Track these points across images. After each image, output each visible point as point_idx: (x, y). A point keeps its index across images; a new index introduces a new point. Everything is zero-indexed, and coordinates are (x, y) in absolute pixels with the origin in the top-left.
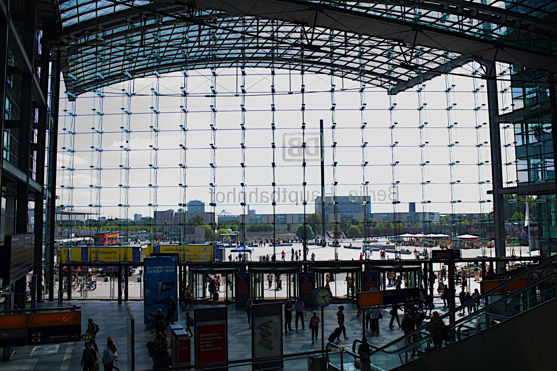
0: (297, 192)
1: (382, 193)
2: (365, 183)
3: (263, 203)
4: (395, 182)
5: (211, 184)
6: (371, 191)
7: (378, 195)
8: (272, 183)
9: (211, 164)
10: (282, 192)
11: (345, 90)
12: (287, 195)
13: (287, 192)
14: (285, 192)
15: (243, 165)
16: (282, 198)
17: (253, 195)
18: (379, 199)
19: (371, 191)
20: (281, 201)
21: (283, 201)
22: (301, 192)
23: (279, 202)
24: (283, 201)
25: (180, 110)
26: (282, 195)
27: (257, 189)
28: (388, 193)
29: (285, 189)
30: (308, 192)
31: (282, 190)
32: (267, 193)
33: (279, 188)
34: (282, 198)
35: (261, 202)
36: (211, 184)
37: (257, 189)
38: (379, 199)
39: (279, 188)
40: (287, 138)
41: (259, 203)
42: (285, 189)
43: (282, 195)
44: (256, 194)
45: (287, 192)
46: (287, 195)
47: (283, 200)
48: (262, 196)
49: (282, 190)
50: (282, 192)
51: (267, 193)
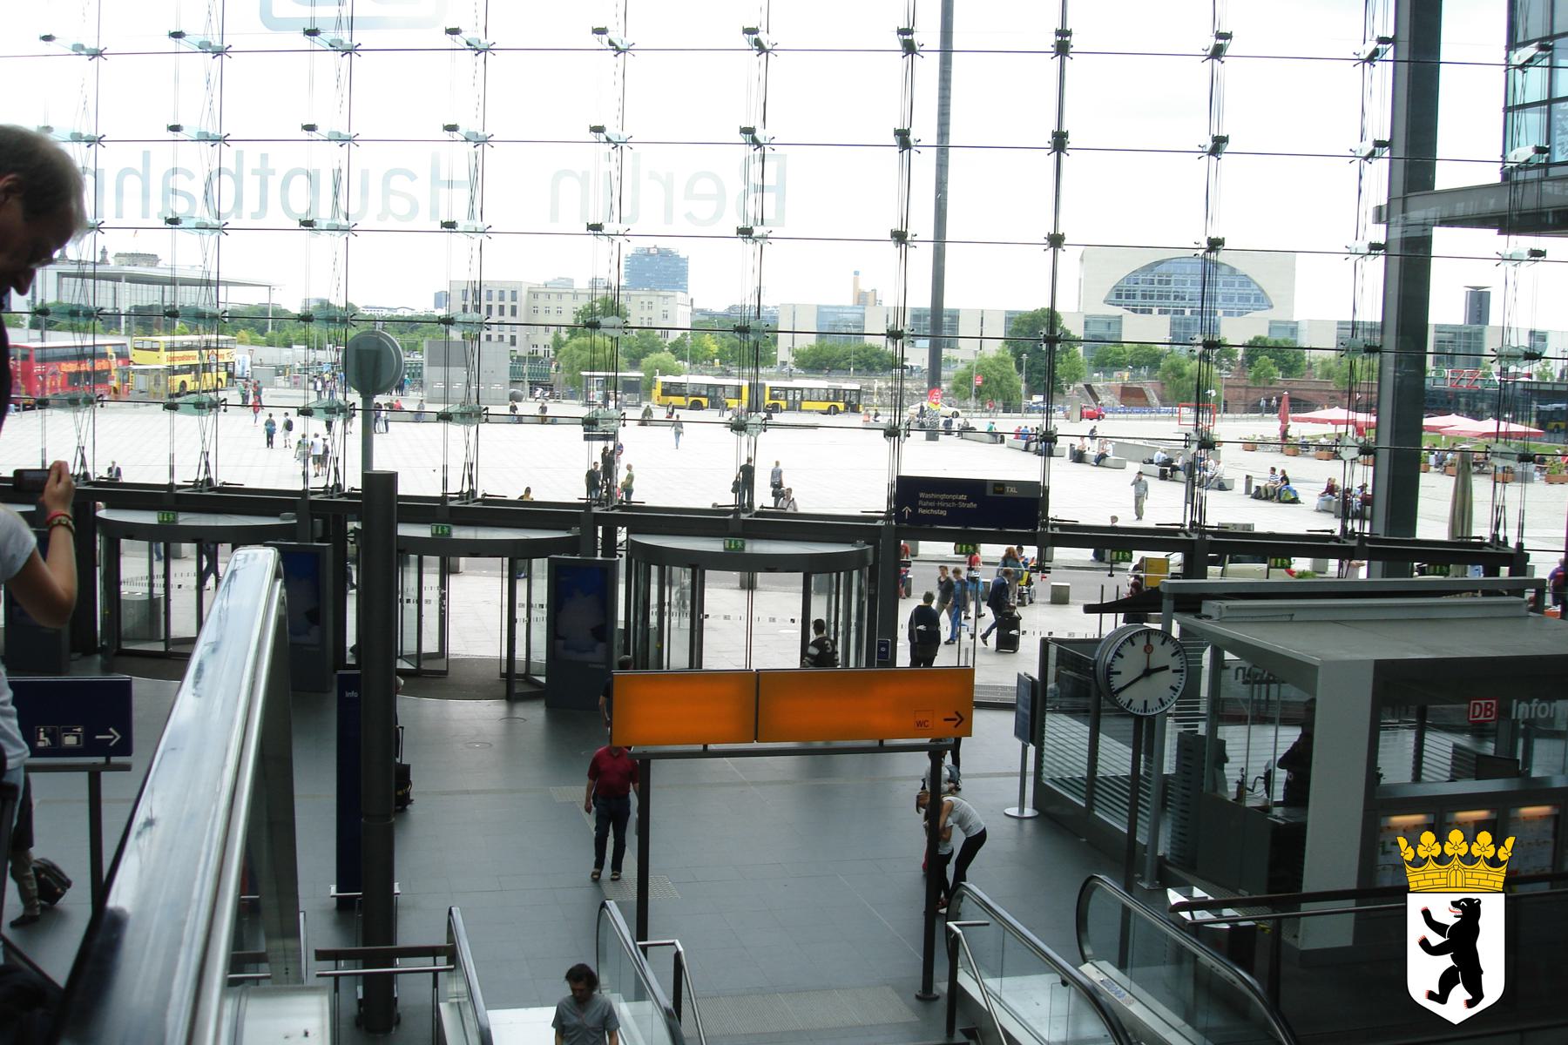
10: (254, 172)
13: (273, 173)
14: (264, 175)
16: (251, 202)
17: (132, 185)
18: (690, 216)
21: (254, 216)
23: (239, 217)
24: (254, 216)
27: (146, 155)
28: (735, 187)
29: (264, 157)
30: (365, 174)
33: (240, 154)
34: (251, 202)
37: (146, 155)
38: (690, 216)
39: (240, 154)
42: (264, 157)
44: (145, 179)
45: (273, 173)
47: (256, 208)
50: (254, 172)
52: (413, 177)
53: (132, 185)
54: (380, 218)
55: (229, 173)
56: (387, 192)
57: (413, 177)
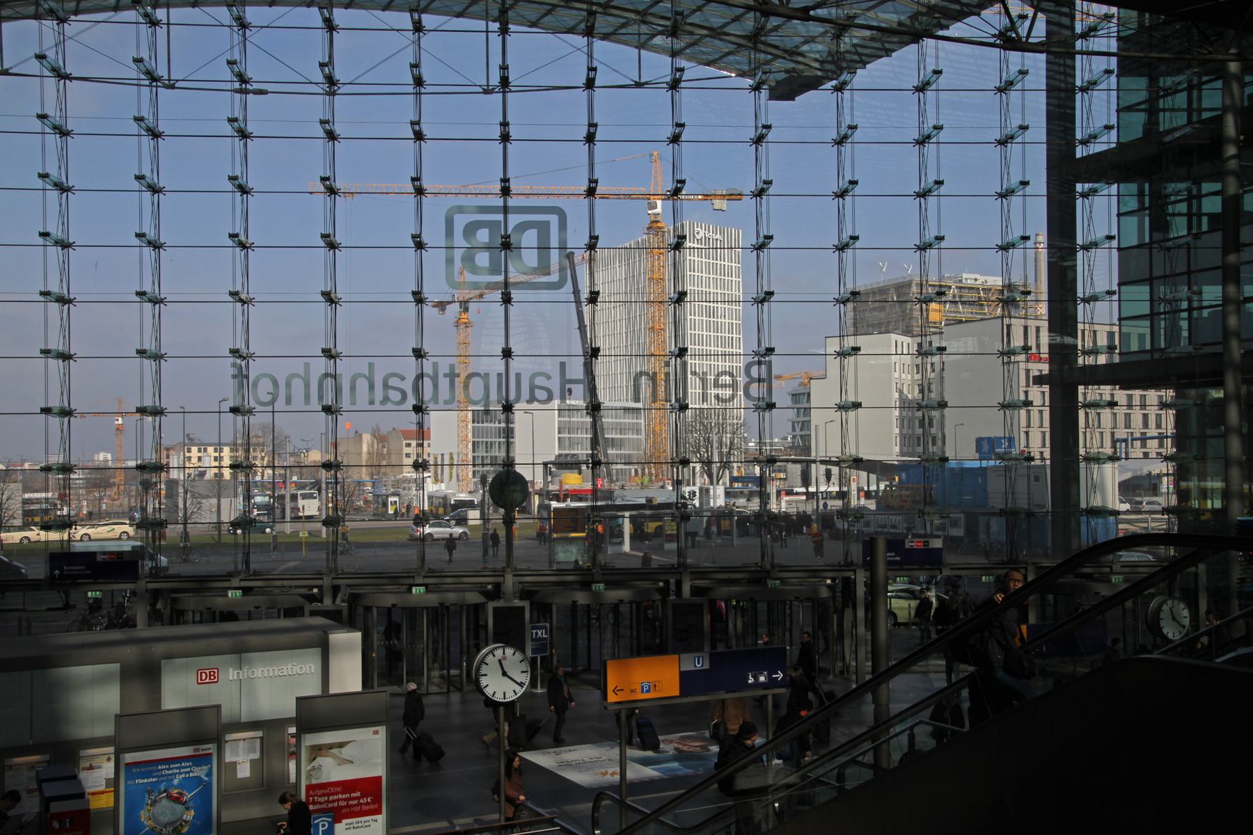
0: (487, 375)
1: (728, 379)
2: (677, 352)
3: (389, 406)
4: (763, 349)
5: (235, 352)
7: (716, 385)
8: (414, 350)
9: (234, 294)
10: (445, 375)
11: (647, 83)
13: (458, 375)
15: (329, 298)
17: (362, 384)
19: (694, 373)
20: (441, 401)
21: (446, 402)
22: (499, 375)
23: (436, 402)
25: (228, 129)
26: (444, 383)
27: (371, 366)
28: (741, 380)
30: (518, 376)
32: (403, 378)
33: (435, 365)
35: (382, 403)
36: (235, 352)
37: (371, 366)
38: (717, 397)
39: (435, 365)
40: (460, 222)
41: (377, 406)
43: (444, 383)
45: (458, 375)
46: (459, 382)
47: (447, 398)
48: (386, 386)
49: (444, 369)
50: (445, 375)
51: (403, 378)
52: (549, 377)
53: (362, 384)
55: (429, 376)
57: (549, 377)
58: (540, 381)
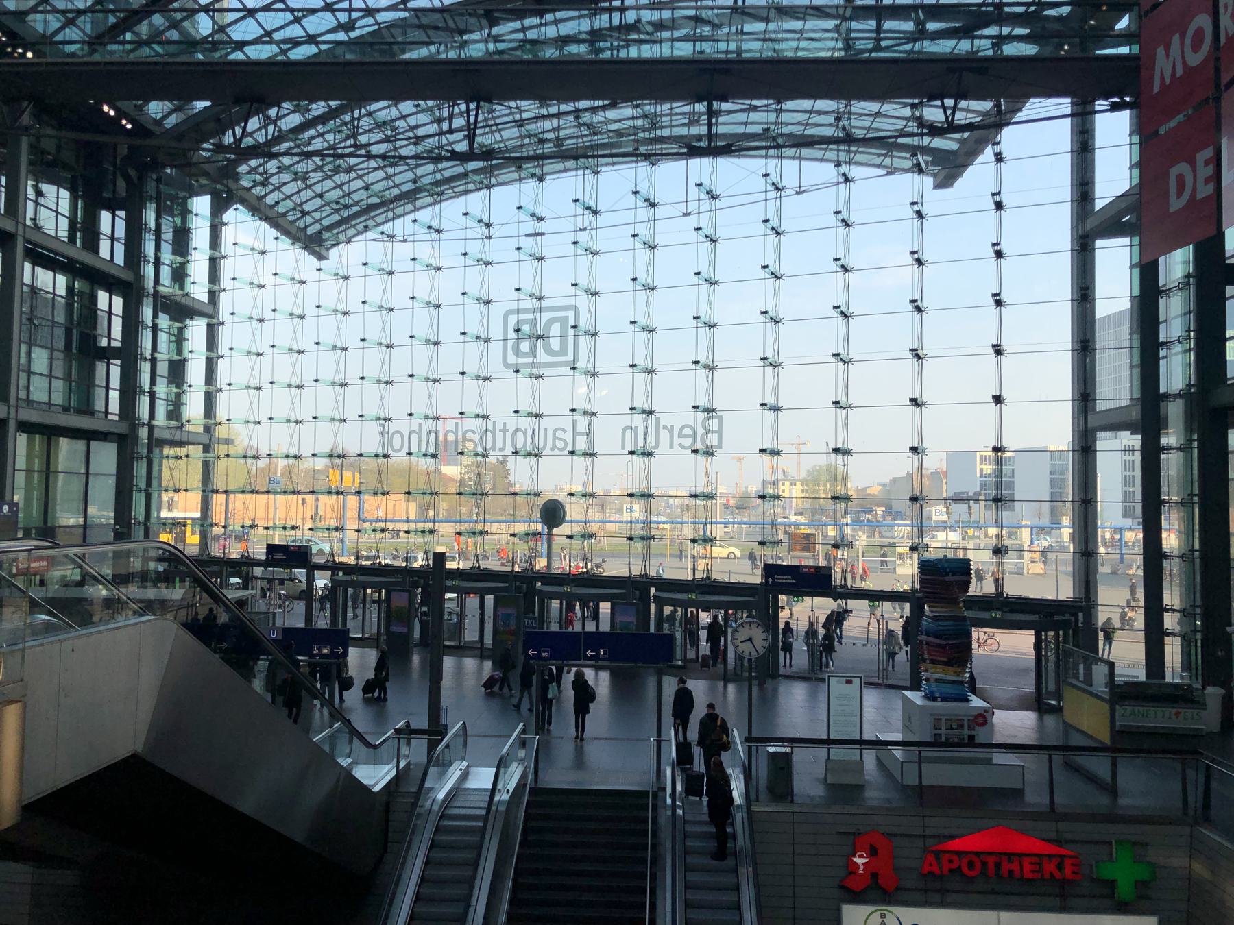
6: (665, 427)
10: (500, 431)
12: (509, 435)
16: (499, 444)
19: (665, 427)
21: (500, 450)
23: (494, 450)
24: (500, 450)
26: (499, 435)
29: (504, 424)
30: (545, 430)
31: (499, 426)
33: (494, 423)
34: (499, 444)
39: (494, 423)
42: (504, 424)
43: (499, 435)
46: (509, 435)
49: (499, 426)
50: (500, 431)
54: (551, 450)
56: (555, 438)
58: (559, 434)
